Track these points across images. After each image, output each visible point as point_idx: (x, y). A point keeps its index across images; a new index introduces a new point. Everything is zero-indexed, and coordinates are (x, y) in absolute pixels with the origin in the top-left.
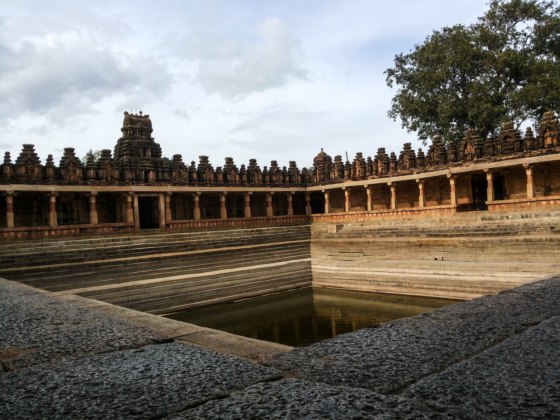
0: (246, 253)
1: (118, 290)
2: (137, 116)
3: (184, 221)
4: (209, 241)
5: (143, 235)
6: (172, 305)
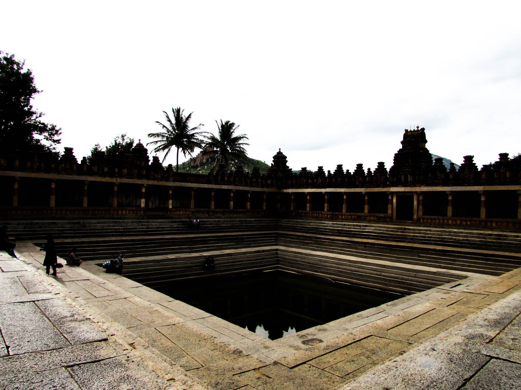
0: (428, 254)
1: (296, 253)
2: (414, 131)
3: (433, 217)
4: (425, 237)
5: (395, 225)
6: (305, 269)
